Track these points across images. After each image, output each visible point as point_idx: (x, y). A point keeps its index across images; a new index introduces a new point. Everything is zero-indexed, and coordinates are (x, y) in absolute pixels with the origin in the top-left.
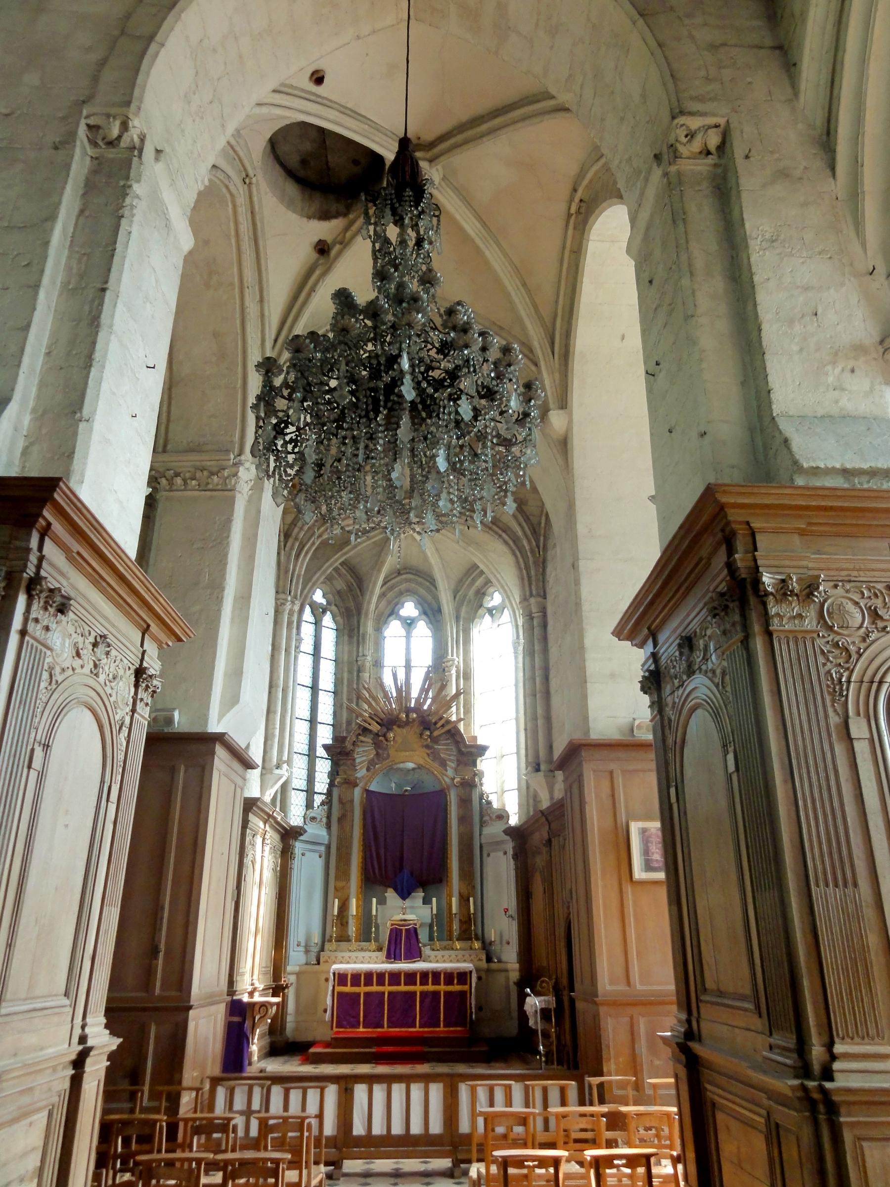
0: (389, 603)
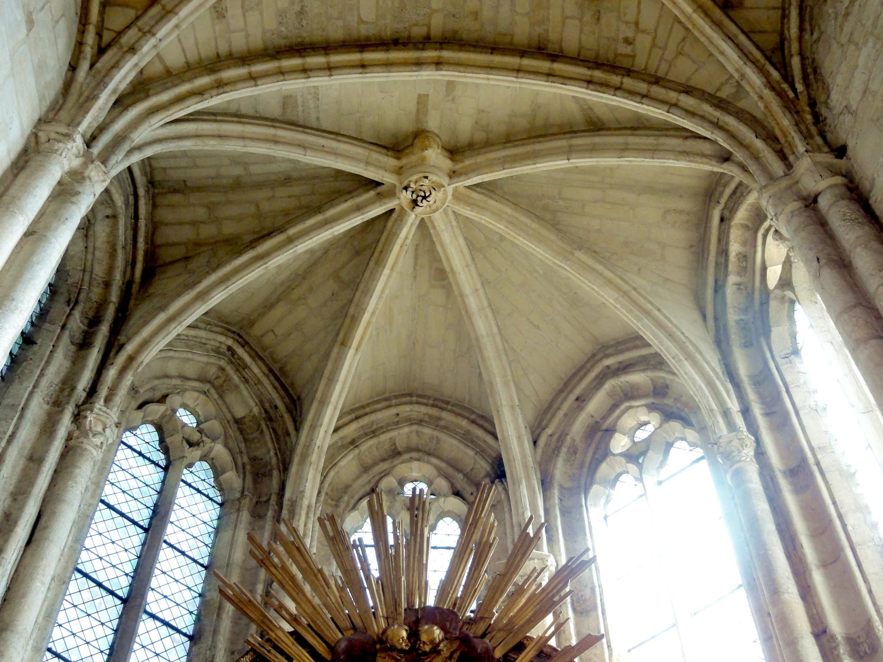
0: (366, 469)
